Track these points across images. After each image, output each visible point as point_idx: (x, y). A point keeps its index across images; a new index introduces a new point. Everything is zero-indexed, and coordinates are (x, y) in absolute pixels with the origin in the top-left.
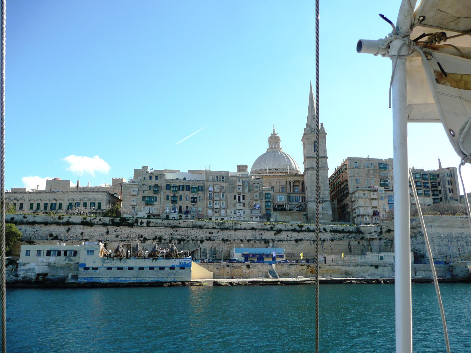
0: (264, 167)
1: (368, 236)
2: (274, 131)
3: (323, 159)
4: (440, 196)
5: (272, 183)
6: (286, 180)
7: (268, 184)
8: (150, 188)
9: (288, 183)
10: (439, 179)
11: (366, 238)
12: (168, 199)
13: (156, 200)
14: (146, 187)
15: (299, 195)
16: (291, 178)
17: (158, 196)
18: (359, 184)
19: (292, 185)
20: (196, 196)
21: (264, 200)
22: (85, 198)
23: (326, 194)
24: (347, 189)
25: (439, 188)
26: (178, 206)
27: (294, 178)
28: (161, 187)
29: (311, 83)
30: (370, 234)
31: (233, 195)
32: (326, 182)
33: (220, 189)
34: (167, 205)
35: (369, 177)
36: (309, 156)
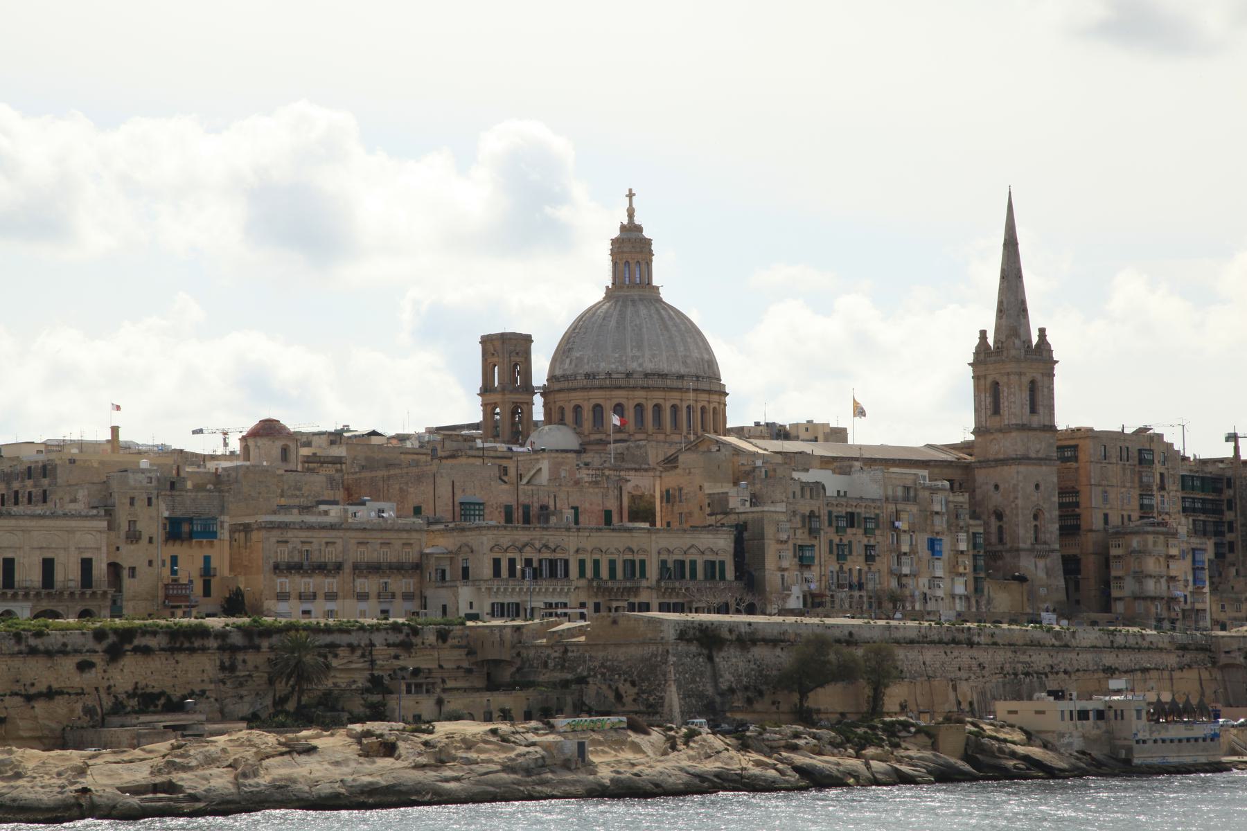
0: (640, 365)
1: (1223, 659)
3: (1048, 435)
4: (1229, 537)
8: (803, 516)
10: (1231, 492)
11: (1221, 664)
12: (831, 552)
14: (798, 518)
18: (1108, 506)
20: (872, 542)
22: (692, 546)
23: (1051, 533)
24: (1078, 516)
25: (1229, 516)
28: (819, 517)
29: (1010, 193)
30: (1229, 655)
35: (1124, 487)
36: (1019, 422)
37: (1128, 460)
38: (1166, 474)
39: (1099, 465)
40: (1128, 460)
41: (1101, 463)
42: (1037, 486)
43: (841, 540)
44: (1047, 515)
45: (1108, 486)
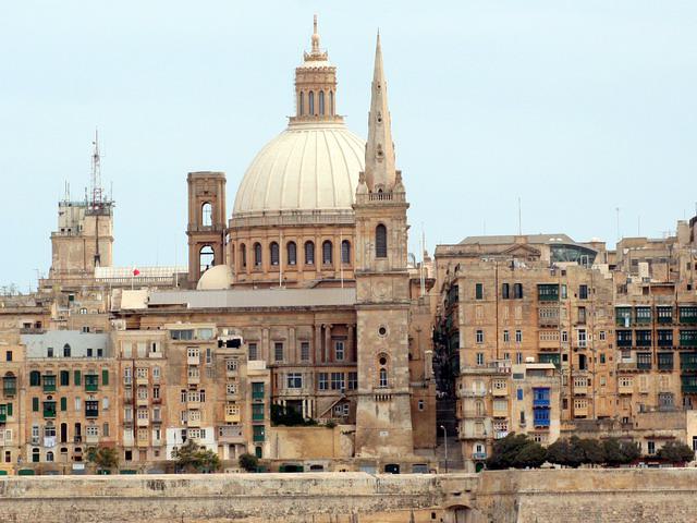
5: (276, 331)
6: (311, 322)
7: (266, 333)
9: (318, 330)
12: (35, 408)
13: (10, 413)
15: (340, 370)
16: (324, 316)
17: (15, 403)
19: (327, 336)
20: (96, 398)
21: (248, 403)
23: (400, 376)
26: (57, 424)
27: (333, 315)
28: (21, 377)
31: (180, 388)
32: (402, 342)
33: (150, 379)
34: (36, 425)
42: (382, 331)
43: (50, 398)
44: (393, 358)
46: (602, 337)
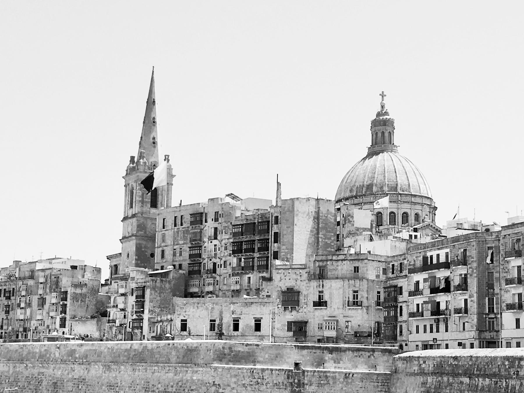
2: (383, 107)
18: (164, 261)
35: (177, 245)
37: (182, 225)
38: (219, 228)
39: (161, 233)
40: (182, 225)
41: (161, 231)
45: (166, 246)
46: (226, 249)
